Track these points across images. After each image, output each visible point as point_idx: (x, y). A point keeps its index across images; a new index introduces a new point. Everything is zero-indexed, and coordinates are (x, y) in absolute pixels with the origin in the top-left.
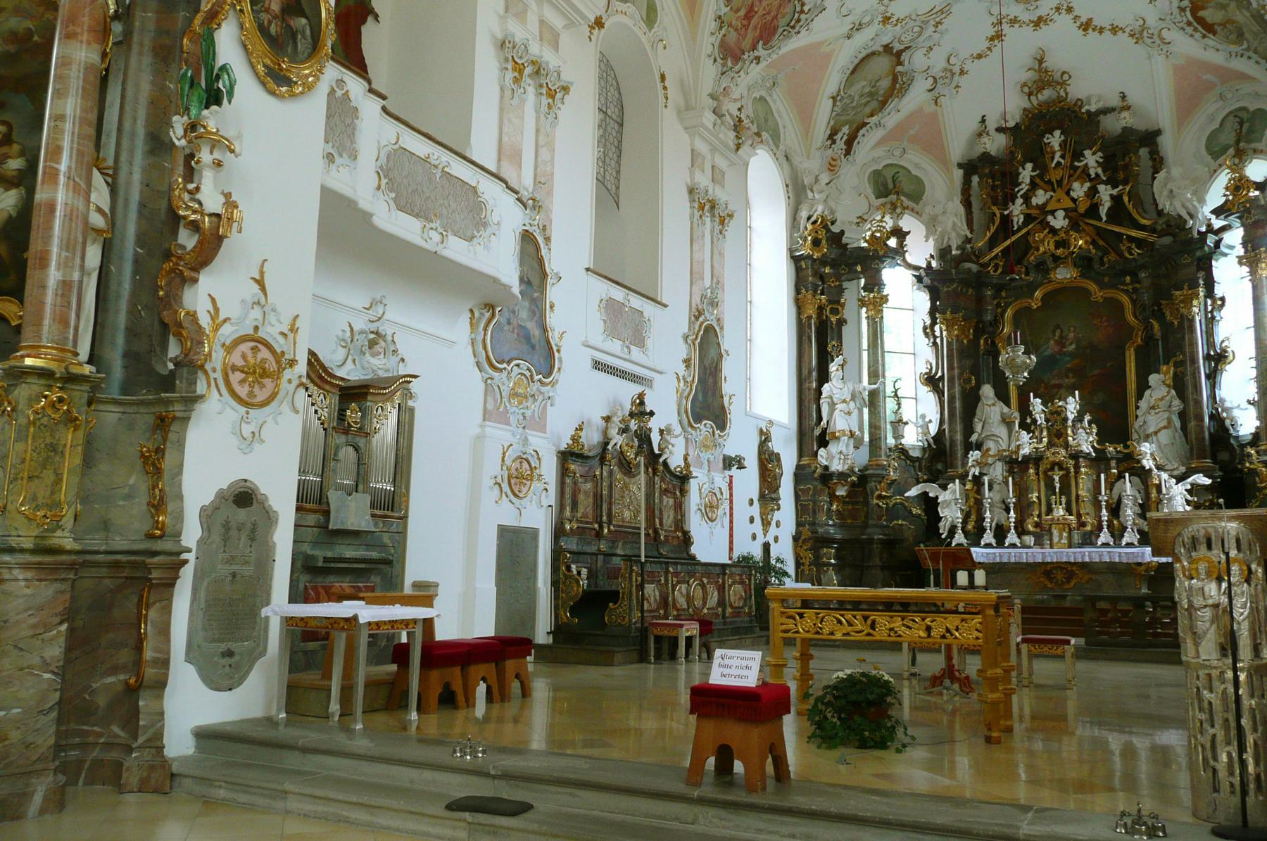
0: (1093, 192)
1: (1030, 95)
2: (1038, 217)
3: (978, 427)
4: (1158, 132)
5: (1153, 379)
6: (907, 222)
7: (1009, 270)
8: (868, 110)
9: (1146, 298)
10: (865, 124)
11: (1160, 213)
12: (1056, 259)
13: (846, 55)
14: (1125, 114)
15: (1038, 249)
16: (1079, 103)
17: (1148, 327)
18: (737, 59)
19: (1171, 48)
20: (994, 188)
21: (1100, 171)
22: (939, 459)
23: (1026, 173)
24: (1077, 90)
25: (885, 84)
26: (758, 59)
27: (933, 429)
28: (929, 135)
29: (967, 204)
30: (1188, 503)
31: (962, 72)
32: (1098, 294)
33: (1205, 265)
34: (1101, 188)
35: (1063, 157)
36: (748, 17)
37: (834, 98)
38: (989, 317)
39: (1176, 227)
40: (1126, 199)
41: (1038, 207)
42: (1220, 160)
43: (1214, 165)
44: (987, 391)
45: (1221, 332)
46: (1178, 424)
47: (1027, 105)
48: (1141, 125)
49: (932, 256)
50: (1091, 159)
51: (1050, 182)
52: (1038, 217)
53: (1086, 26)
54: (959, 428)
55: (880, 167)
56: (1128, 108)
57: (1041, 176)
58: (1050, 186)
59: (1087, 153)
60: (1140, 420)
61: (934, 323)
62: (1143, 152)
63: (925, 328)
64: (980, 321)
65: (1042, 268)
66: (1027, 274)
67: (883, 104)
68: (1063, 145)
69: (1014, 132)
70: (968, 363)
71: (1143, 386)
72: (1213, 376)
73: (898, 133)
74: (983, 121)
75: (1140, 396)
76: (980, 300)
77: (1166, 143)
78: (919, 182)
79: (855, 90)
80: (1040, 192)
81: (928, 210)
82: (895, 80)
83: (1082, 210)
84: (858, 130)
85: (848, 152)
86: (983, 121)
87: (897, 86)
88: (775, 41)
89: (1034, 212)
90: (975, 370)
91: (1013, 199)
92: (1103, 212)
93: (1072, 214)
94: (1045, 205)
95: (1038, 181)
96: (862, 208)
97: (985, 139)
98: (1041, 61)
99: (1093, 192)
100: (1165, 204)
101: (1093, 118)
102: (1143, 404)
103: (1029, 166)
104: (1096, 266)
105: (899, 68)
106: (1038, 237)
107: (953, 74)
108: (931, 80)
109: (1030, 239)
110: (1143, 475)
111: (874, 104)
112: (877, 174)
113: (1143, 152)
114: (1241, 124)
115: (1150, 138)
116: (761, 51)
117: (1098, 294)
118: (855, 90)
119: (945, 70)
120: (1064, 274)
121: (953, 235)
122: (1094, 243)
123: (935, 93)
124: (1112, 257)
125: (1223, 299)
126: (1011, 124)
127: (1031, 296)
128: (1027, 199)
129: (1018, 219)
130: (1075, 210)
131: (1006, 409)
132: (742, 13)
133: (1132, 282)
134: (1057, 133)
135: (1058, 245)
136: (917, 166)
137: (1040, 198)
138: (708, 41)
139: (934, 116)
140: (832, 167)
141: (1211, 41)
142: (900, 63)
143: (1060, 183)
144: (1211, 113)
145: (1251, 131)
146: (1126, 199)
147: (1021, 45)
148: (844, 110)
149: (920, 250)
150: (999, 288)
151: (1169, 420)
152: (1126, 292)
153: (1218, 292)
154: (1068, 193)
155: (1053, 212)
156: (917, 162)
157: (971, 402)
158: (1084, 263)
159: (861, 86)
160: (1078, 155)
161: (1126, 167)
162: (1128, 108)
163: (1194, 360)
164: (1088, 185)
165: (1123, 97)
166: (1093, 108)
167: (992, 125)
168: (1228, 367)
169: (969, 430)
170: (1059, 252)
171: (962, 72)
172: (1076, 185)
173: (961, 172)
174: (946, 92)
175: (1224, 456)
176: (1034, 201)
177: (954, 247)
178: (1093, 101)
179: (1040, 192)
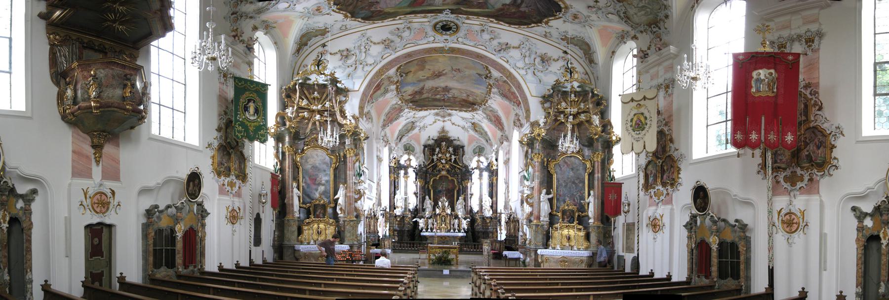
2: (439, 160)
6: (412, 157)
13: (404, 123)
22: (417, 212)
23: (437, 150)
28: (417, 138)
32: (450, 178)
33: (471, 175)
39: (466, 167)
50: (451, 149)
52: (439, 160)
58: (442, 153)
65: (439, 171)
71: (458, 199)
77: (466, 148)
87: (413, 128)
101: (452, 141)
107: (424, 127)
110: (459, 219)
115: (463, 147)
117: (450, 178)
120: (444, 173)
137: (440, 155)
140: (396, 145)
144: (474, 145)
147: (439, 125)
149: (414, 163)
156: (413, 143)
157: (423, 200)
158: (448, 171)
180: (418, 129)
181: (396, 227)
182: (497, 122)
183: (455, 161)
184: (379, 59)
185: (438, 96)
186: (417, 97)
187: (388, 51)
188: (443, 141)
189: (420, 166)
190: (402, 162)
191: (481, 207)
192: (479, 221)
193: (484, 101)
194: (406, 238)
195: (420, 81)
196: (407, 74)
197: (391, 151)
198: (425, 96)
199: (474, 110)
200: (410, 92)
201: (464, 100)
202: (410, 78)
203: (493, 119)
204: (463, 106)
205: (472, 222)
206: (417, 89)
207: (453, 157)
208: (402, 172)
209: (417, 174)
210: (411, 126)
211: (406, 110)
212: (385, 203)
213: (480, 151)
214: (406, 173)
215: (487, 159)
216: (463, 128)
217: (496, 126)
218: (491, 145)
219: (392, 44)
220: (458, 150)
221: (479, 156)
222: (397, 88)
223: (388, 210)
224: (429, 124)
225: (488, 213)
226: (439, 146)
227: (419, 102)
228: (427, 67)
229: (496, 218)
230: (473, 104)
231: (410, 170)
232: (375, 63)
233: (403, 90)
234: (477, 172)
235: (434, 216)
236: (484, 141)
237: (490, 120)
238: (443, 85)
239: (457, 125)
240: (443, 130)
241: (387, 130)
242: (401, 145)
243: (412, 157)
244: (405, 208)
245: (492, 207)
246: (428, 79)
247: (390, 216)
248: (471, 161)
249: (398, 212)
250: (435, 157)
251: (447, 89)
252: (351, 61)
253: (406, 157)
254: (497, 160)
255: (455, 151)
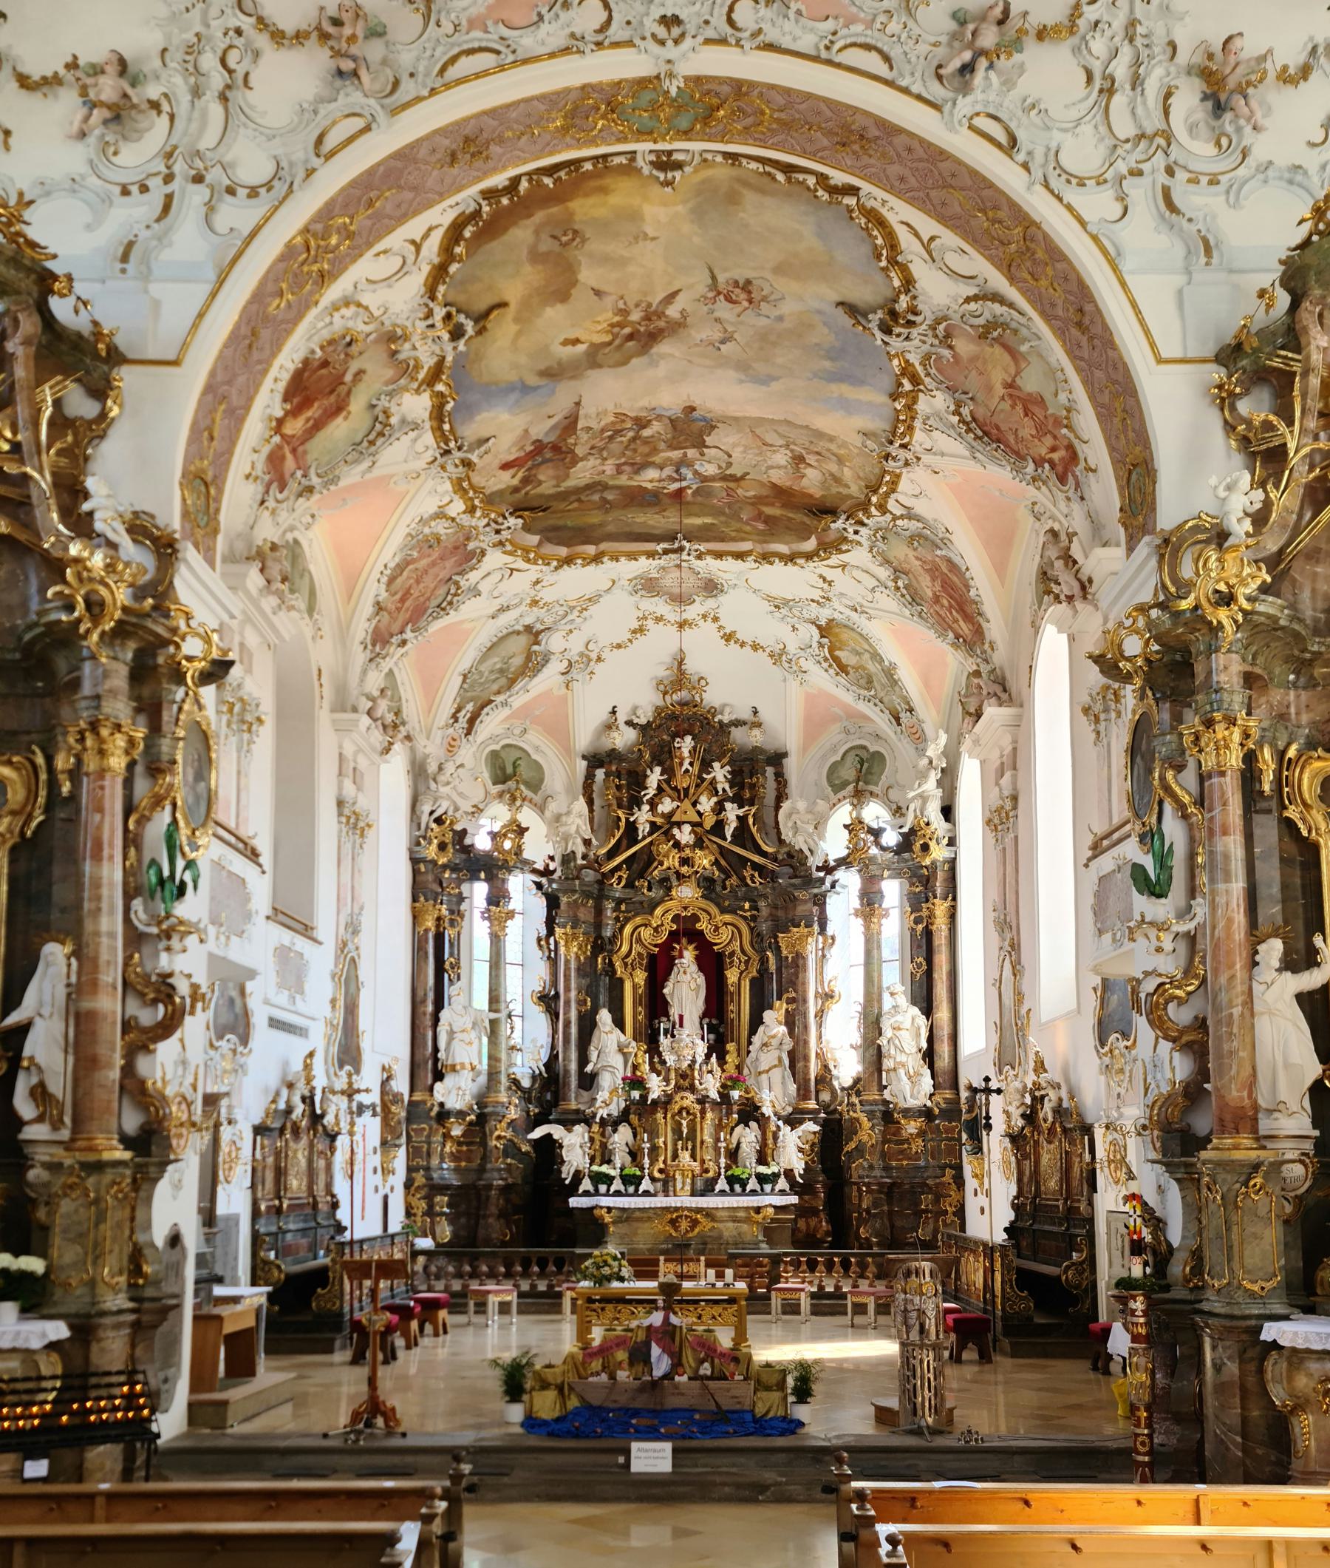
0: (719, 808)
1: (665, 693)
2: (665, 827)
3: (593, 1055)
4: (785, 755)
5: (768, 1015)
6: (527, 816)
7: (630, 885)
8: (495, 687)
9: (764, 927)
10: (491, 702)
11: (781, 842)
12: (679, 876)
13: (486, 633)
14: (756, 732)
15: (661, 863)
16: (713, 711)
17: (764, 961)
18: (386, 642)
19: (806, 677)
20: (619, 788)
21: (727, 787)
22: (551, 1093)
23: (654, 777)
24: (711, 697)
25: (517, 661)
26: (404, 643)
27: (544, 1056)
29: (590, 802)
30: (800, 1150)
31: (599, 659)
34: (728, 805)
35: (691, 764)
36: (403, 600)
37: (465, 676)
38: (608, 933)
39: (795, 860)
40: (751, 821)
41: (663, 815)
42: (840, 795)
43: (834, 798)
44: (604, 1016)
45: (831, 970)
46: (787, 1062)
47: (660, 703)
48: (771, 746)
49: (552, 858)
50: (720, 773)
51: (675, 789)
52: (665, 827)
53: (728, 637)
54: (574, 1055)
55: (497, 747)
56: (759, 725)
57: (668, 782)
58: (681, 794)
59: (716, 765)
60: (753, 1055)
61: (550, 932)
62: (770, 771)
63: (539, 940)
64: (599, 937)
65: (665, 884)
66: (650, 889)
67: (512, 682)
68: (693, 751)
69: (644, 729)
70: (585, 982)
71: (756, 1022)
72: (820, 1014)
73: (525, 711)
74: (614, 712)
75: (753, 1031)
76: (599, 911)
77: (792, 767)
78: (538, 767)
79: (485, 667)
80: (667, 800)
81: (552, 807)
82: (528, 658)
83: (709, 822)
84: (482, 708)
85: (468, 733)
86: (614, 712)
87: (533, 664)
88: (422, 624)
89: (659, 821)
90: (591, 991)
91: (639, 803)
92: (729, 832)
93: (698, 830)
94: (672, 813)
95: (665, 786)
96: (477, 794)
97: (615, 734)
98: (681, 663)
99: (719, 808)
100: (787, 835)
102: (757, 1040)
103: (658, 770)
104: (718, 889)
105: (535, 648)
106: (664, 848)
108: (566, 663)
109: (654, 848)
111: (503, 681)
112: (494, 755)
113: (770, 771)
114: (862, 762)
115: (777, 759)
116: (409, 635)
118: (485, 667)
119: (581, 654)
121: (579, 841)
122: (716, 863)
123: (569, 677)
124: (734, 880)
125: (833, 938)
126: (643, 721)
127: (651, 913)
128: (653, 805)
129: (643, 828)
130: (700, 825)
131: (623, 1038)
132: (398, 597)
133: (751, 908)
134: (688, 739)
135: (685, 861)
136: (537, 748)
137: (666, 806)
138: (362, 627)
139: (565, 699)
140: (451, 748)
141: (842, 679)
142: (538, 643)
143: (686, 790)
145: (869, 772)
146: (751, 821)
148: (472, 686)
150: (619, 902)
151: (780, 1059)
152: (745, 918)
153: (830, 931)
154: (694, 804)
155: (679, 824)
156: (540, 747)
158: (707, 885)
159: (495, 662)
160: (706, 766)
161: (753, 786)
162: (759, 725)
163: (805, 1001)
164: (715, 799)
165: (755, 713)
166: (726, 719)
167: (622, 717)
168: (834, 1007)
169: (583, 1060)
170: (684, 870)
171: (599, 659)
172: (703, 799)
173: (584, 763)
174: (579, 677)
175: (825, 1096)
176: (660, 809)
177: (579, 856)
178: (727, 710)
179: (667, 800)
180: (555, 666)
181: (445, 1171)
182: (948, 601)
183: (742, 834)
184: (300, 150)
185: (649, 478)
186: (547, 483)
187: (352, 97)
188: (683, 724)
189: (568, 859)
190: (482, 842)
191: (875, 1057)
192: (868, 1132)
193: (880, 485)
194: (494, 1227)
195: (555, 373)
196: (481, 318)
197: (420, 775)
198: (582, 473)
199: (830, 546)
200: (506, 447)
201: (781, 494)
202: (504, 351)
203: (927, 586)
204: (773, 528)
205: (833, 1135)
206: (542, 430)
207: (732, 812)
208: (479, 891)
209: (553, 903)
210: (525, 652)
211: (495, 559)
212: (387, 1041)
213: (861, 773)
214: (497, 897)
215: (898, 811)
216: (777, 657)
217: (943, 626)
218: (919, 739)
219: (374, 51)
220: (756, 772)
221: (859, 797)
222: (438, 414)
223: (401, 1084)
224: (616, 639)
225: (911, 1087)
226: (664, 756)
227: (557, 508)
228: (588, 275)
229: (952, 1111)
230: (826, 510)
231: (518, 885)
232: (279, 186)
233: (470, 431)
234: (850, 880)
235: (640, 1111)
236: (882, 721)
237: (913, 597)
238: (670, 400)
239: (750, 636)
240: (679, 677)
241: (403, 663)
242: (472, 754)
243: (527, 816)
244: (493, 1075)
245: (929, 1056)
246: (594, 358)
247: (412, 1119)
248: (819, 825)
249: (455, 1093)
250: (643, 817)
251: (691, 429)
252: (139, 154)
253: (497, 816)
254: (948, 812)
255: (737, 778)
